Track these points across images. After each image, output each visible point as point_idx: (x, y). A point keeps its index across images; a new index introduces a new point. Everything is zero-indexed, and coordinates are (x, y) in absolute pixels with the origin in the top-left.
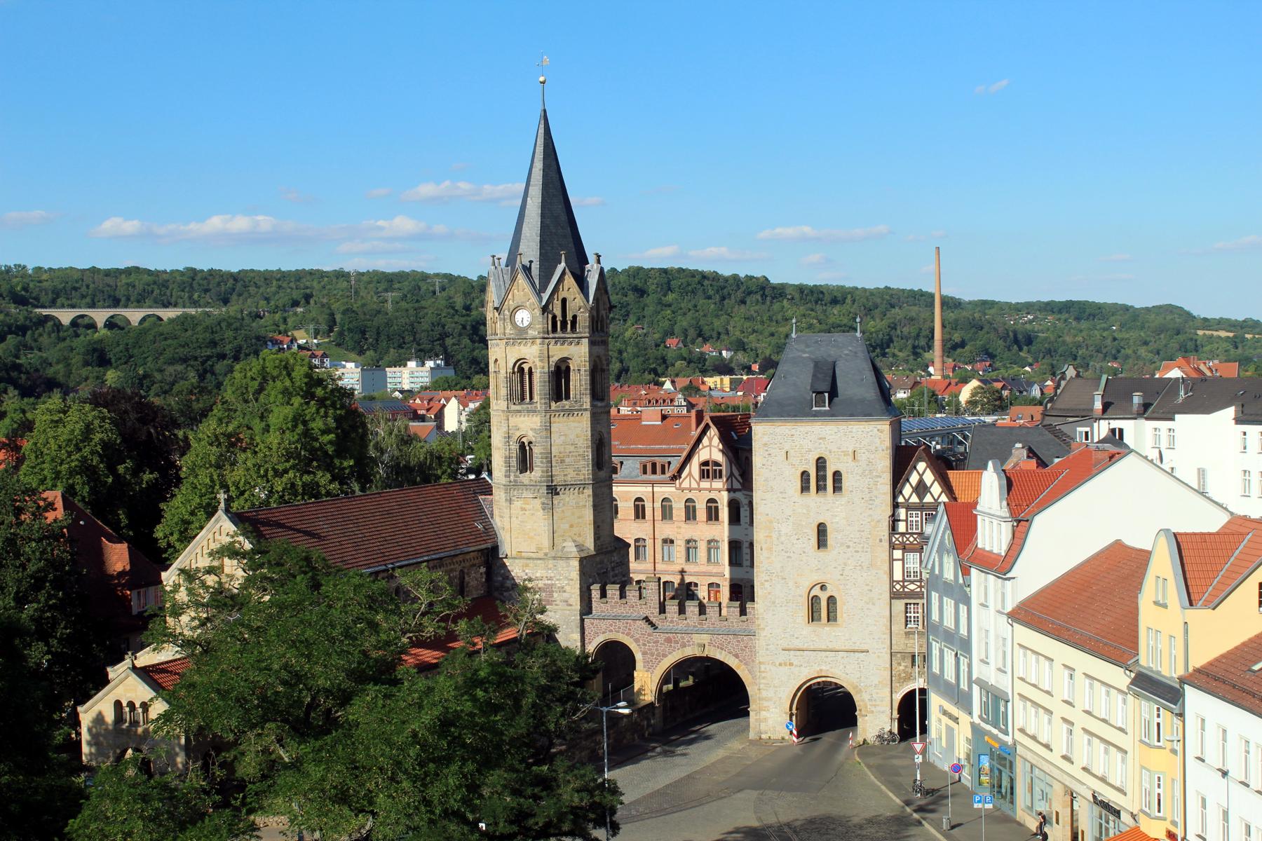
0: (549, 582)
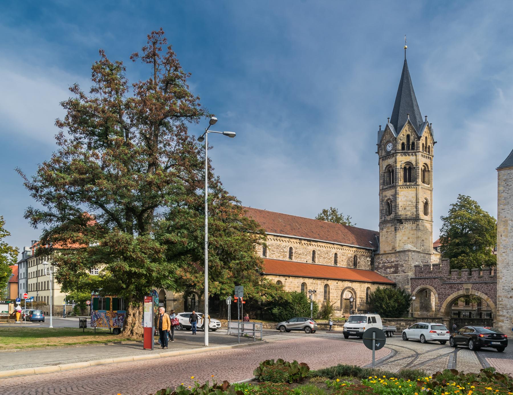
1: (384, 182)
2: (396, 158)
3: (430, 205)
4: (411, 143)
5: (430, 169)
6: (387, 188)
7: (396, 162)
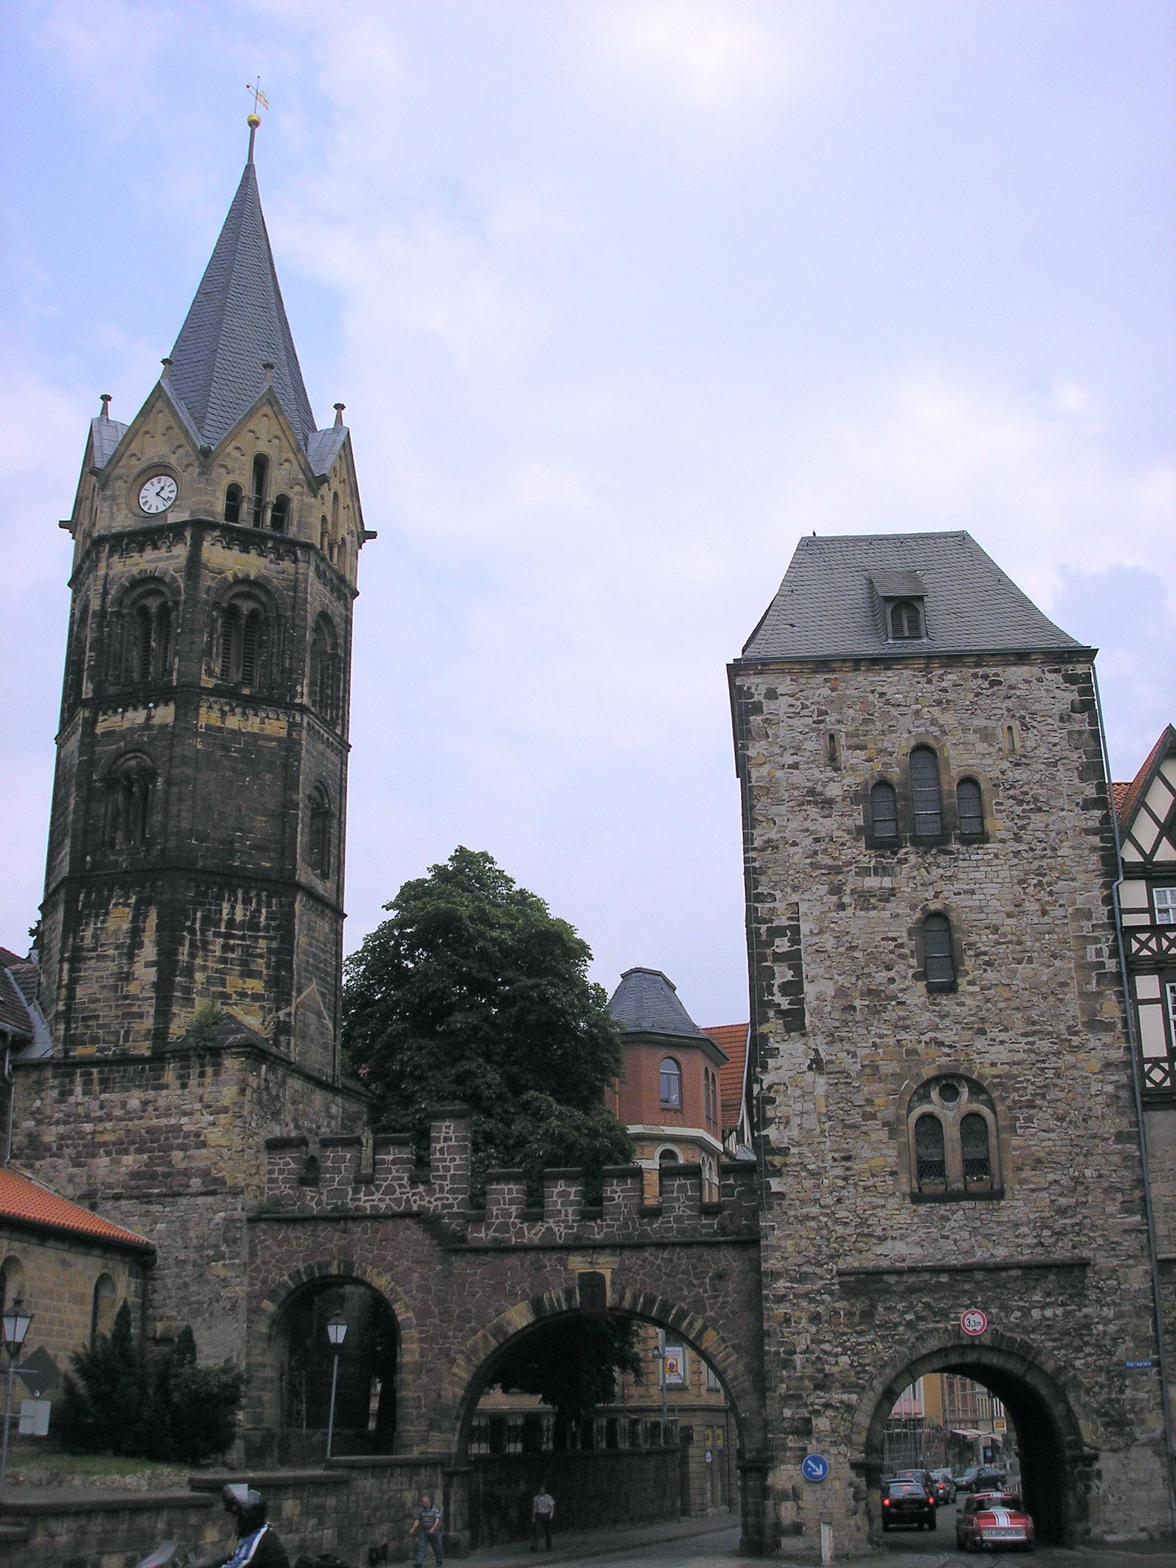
0: (164, 1121)
4: (271, 498)
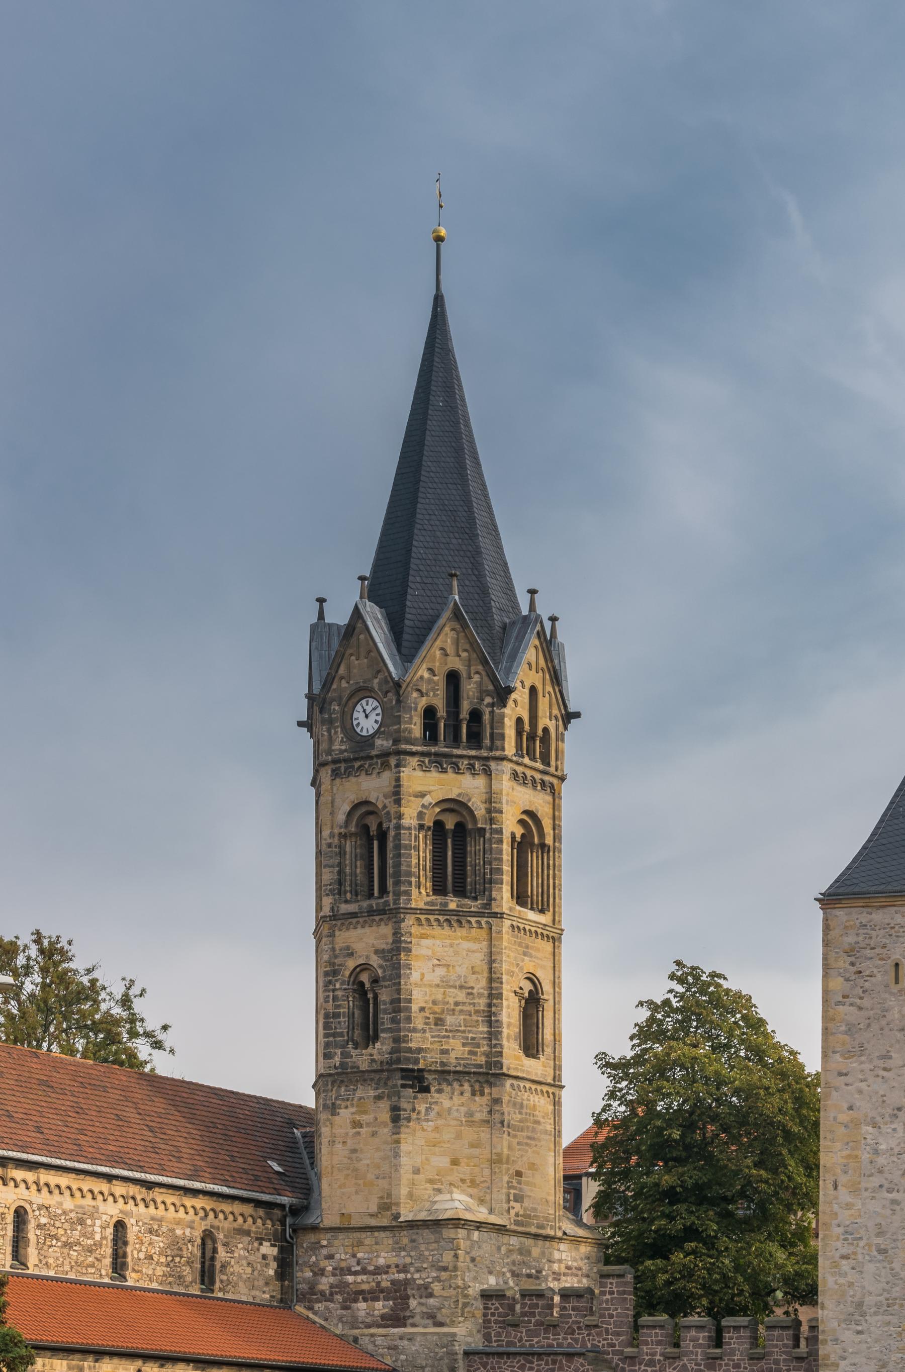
1: (340, 883)
2: (398, 779)
3: (548, 1006)
4: (464, 714)
5: (549, 840)
6: (353, 915)
7: (396, 795)
